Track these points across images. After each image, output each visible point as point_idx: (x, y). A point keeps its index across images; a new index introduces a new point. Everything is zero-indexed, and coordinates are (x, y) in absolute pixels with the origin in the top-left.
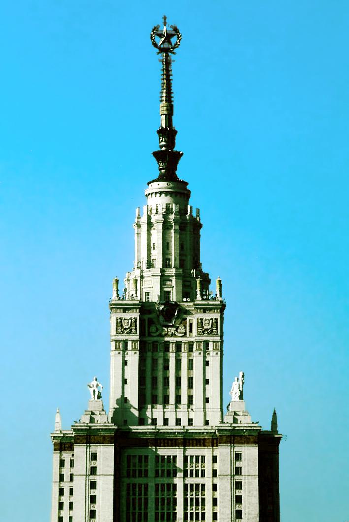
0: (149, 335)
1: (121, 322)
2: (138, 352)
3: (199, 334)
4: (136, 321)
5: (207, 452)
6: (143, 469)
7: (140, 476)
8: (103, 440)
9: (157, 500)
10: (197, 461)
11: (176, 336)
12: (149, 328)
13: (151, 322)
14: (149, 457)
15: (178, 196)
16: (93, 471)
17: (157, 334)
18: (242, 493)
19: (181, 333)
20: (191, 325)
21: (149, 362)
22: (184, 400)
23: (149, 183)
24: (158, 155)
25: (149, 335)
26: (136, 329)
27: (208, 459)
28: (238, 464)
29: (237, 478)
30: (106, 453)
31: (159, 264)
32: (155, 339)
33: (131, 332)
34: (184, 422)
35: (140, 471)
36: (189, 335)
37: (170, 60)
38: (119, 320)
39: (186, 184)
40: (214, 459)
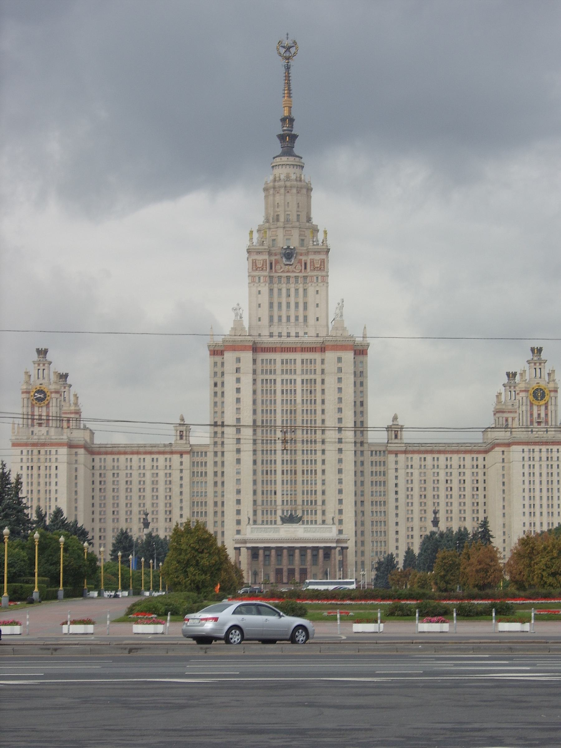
0: (276, 272)
2: (267, 284)
3: (311, 270)
4: (266, 262)
5: (317, 356)
6: (273, 369)
7: (271, 373)
9: (283, 391)
11: (295, 272)
12: (275, 267)
13: (277, 262)
14: (277, 360)
15: (295, 167)
16: (238, 370)
17: (281, 270)
18: (342, 385)
19: (298, 270)
20: (305, 264)
21: (276, 291)
22: (301, 319)
23: (274, 158)
24: (282, 137)
26: (266, 267)
27: (319, 361)
28: (340, 365)
29: (340, 375)
31: (282, 219)
32: (280, 274)
34: (301, 334)
36: (304, 271)
37: (290, 65)
38: (254, 261)
39: (301, 158)
40: (323, 361)
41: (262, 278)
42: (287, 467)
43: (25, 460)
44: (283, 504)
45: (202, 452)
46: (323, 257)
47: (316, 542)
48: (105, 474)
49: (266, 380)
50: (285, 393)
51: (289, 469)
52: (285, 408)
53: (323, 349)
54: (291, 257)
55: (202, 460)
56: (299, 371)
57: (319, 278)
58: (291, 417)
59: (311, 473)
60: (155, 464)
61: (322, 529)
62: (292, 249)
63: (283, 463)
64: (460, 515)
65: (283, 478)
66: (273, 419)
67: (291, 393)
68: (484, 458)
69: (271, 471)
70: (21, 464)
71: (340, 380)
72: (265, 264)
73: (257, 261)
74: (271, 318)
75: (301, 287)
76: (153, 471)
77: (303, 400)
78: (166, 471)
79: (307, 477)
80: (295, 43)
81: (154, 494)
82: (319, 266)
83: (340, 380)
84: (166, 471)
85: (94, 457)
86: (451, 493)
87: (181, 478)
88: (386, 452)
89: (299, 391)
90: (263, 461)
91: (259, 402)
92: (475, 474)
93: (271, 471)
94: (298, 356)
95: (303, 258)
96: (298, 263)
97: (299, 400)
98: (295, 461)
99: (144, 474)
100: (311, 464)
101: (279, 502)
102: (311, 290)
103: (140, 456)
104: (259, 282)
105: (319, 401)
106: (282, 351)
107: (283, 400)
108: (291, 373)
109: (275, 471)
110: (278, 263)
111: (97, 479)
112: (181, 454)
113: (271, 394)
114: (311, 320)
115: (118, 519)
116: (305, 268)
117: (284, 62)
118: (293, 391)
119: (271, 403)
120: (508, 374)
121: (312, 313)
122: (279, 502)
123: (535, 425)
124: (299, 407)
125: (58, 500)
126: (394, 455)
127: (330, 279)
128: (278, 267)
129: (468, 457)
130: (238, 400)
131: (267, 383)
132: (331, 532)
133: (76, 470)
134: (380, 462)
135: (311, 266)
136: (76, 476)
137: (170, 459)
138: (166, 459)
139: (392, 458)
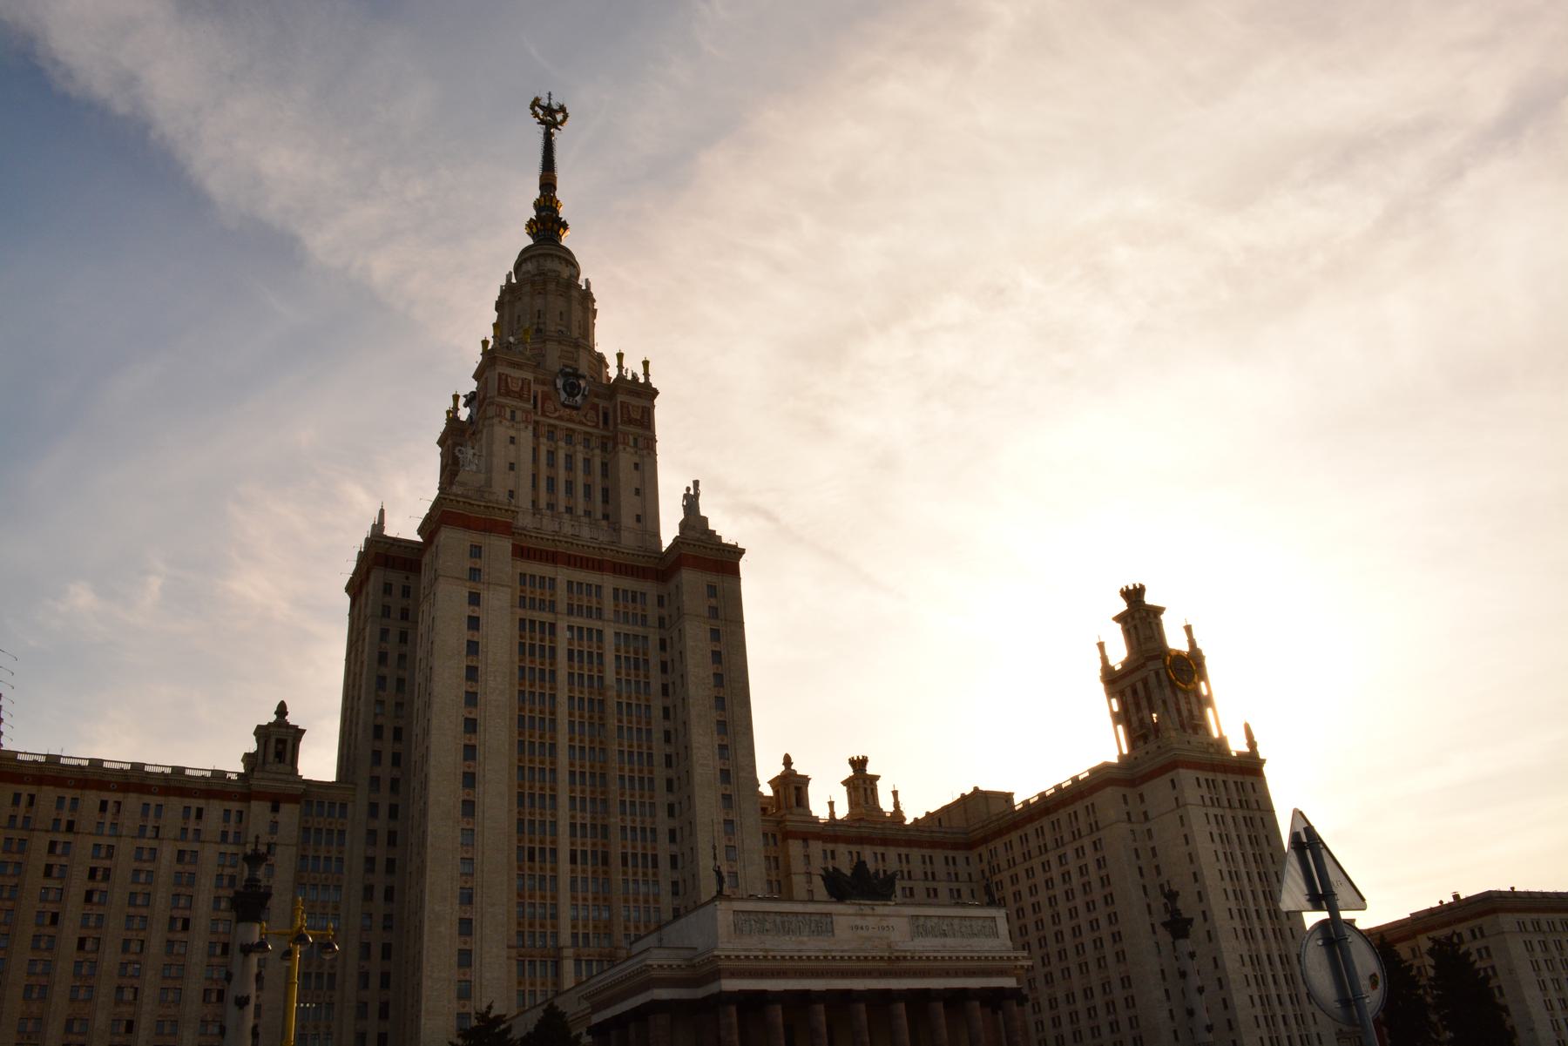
0: (544, 414)
1: (506, 380)
5: (650, 589)
6: (548, 598)
9: (571, 652)
10: (634, 600)
11: (586, 425)
12: (542, 407)
16: (475, 573)
17: (557, 414)
19: (591, 421)
27: (652, 600)
32: (552, 421)
33: (521, 397)
35: (542, 601)
38: (504, 377)
41: (519, 415)
42: (583, 844)
44: (575, 944)
45: (332, 805)
46: (643, 403)
47: (957, 974)
48: (22, 841)
49: (532, 622)
50: (576, 660)
51: (589, 849)
52: (577, 695)
54: (577, 395)
55: (330, 824)
57: (640, 439)
58: (591, 717)
59: (645, 866)
61: (967, 923)
63: (573, 834)
65: (573, 871)
66: (547, 717)
67: (591, 662)
68: (967, 858)
69: (542, 850)
72: (526, 389)
73: (509, 380)
76: (182, 846)
77: (619, 681)
79: (635, 874)
80: (562, 109)
81: (177, 913)
82: (639, 418)
84: (223, 848)
88: (779, 837)
89: (609, 658)
93: (542, 850)
94: (609, 582)
96: (591, 409)
97: (610, 676)
98: (605, 827)
99: (153, 850)
100: (644, 839)
101: (565, 937)
102: (625, 459)
103: (147, 799)
104: (513, 418)
105: (656, 686)
106: (569, 564)
107: (571, 675)
108: (590, 616)
109: (554, 852)
110: (550, 399)
112: (276, 802)
113: (542, 656)
114: (627, 520)
116: (606, 422)
117: (541, 129)
118: (595, 656)
119: (542, 679)
120: (853, 762)
121: (628, 506)
122: (565, 937)
123: (1190, 731)
124: (612, 694)
126: (801, 841)
127: (659, 447)
128: (549, 406)
129: (939, 855)
130: (473, 648)
131: (532, 630)
132: (996, 935)
135: (622, 413)
139: (795, 847)
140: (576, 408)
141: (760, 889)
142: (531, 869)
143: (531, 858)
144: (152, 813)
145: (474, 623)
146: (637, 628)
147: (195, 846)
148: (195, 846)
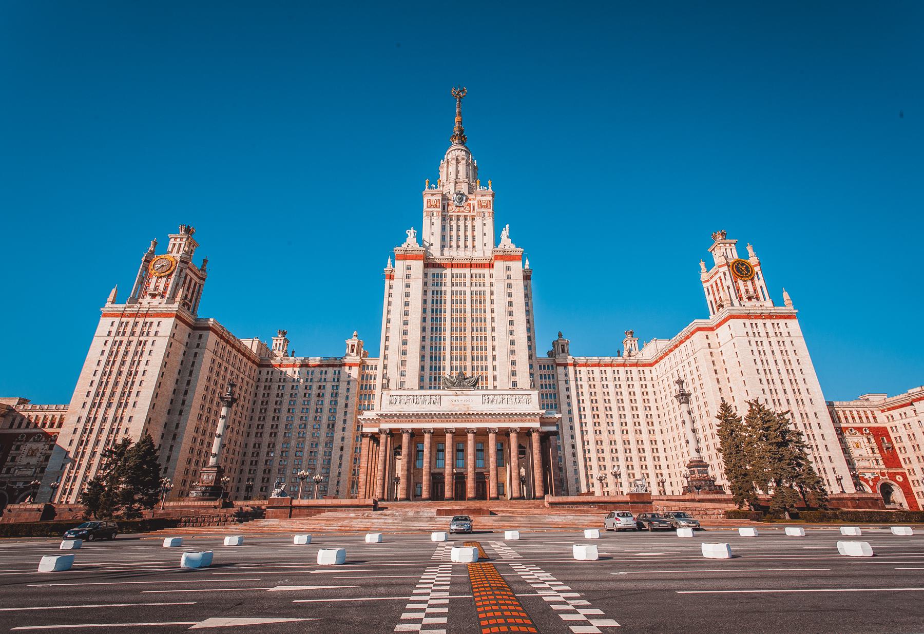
5: (486, 271)
8: (416, 258)
10: (480, 277)
16: (408, 277)
18: (512, 290)
20: (474, 207)
25: (448, 212)
27: (487, 276)
28: (509, 273)
30: (418, 266)
32: (451, 214)
40: (491, 276)
43: (113, 334)
48: (270, 386)
49: (437, 291)
53: (491, 266)
56: (468, 284)
60: (323, 377)
62: (461, 194)
64: (636, 427)
70: (107, 338)
71: (509, 286)
74: (443, 247)
75: (469, 224)
76: (320, 384)
78: (333, 384)
81: (318, 407)
83: (509, 286)
84: (333, 384)
85: (262, 369)
86: (623, 405)
87: (348, 390)
88: (554, 366)
90: (431, 367)
91: (429, 310)
92: (644, 386)
94: (467, 271)
95: (472, 202)
105: (488, 310)
111: (261, 391)
115: (275, 434)
124: (468, 315)
125: (144, 384)
133: (196, 354)
134: (549, 375)
136: (194, 363)
137: (339, 372)
138: (335, 371)
139: (561, 370)
140: (460, 207)
141: (528, 386)
142: (435, 384)
143: (435, 380)
144: (310, 373)
145: (407, 295)
146: (480, 288)
147: (324, 384)
148: (324, 384)
